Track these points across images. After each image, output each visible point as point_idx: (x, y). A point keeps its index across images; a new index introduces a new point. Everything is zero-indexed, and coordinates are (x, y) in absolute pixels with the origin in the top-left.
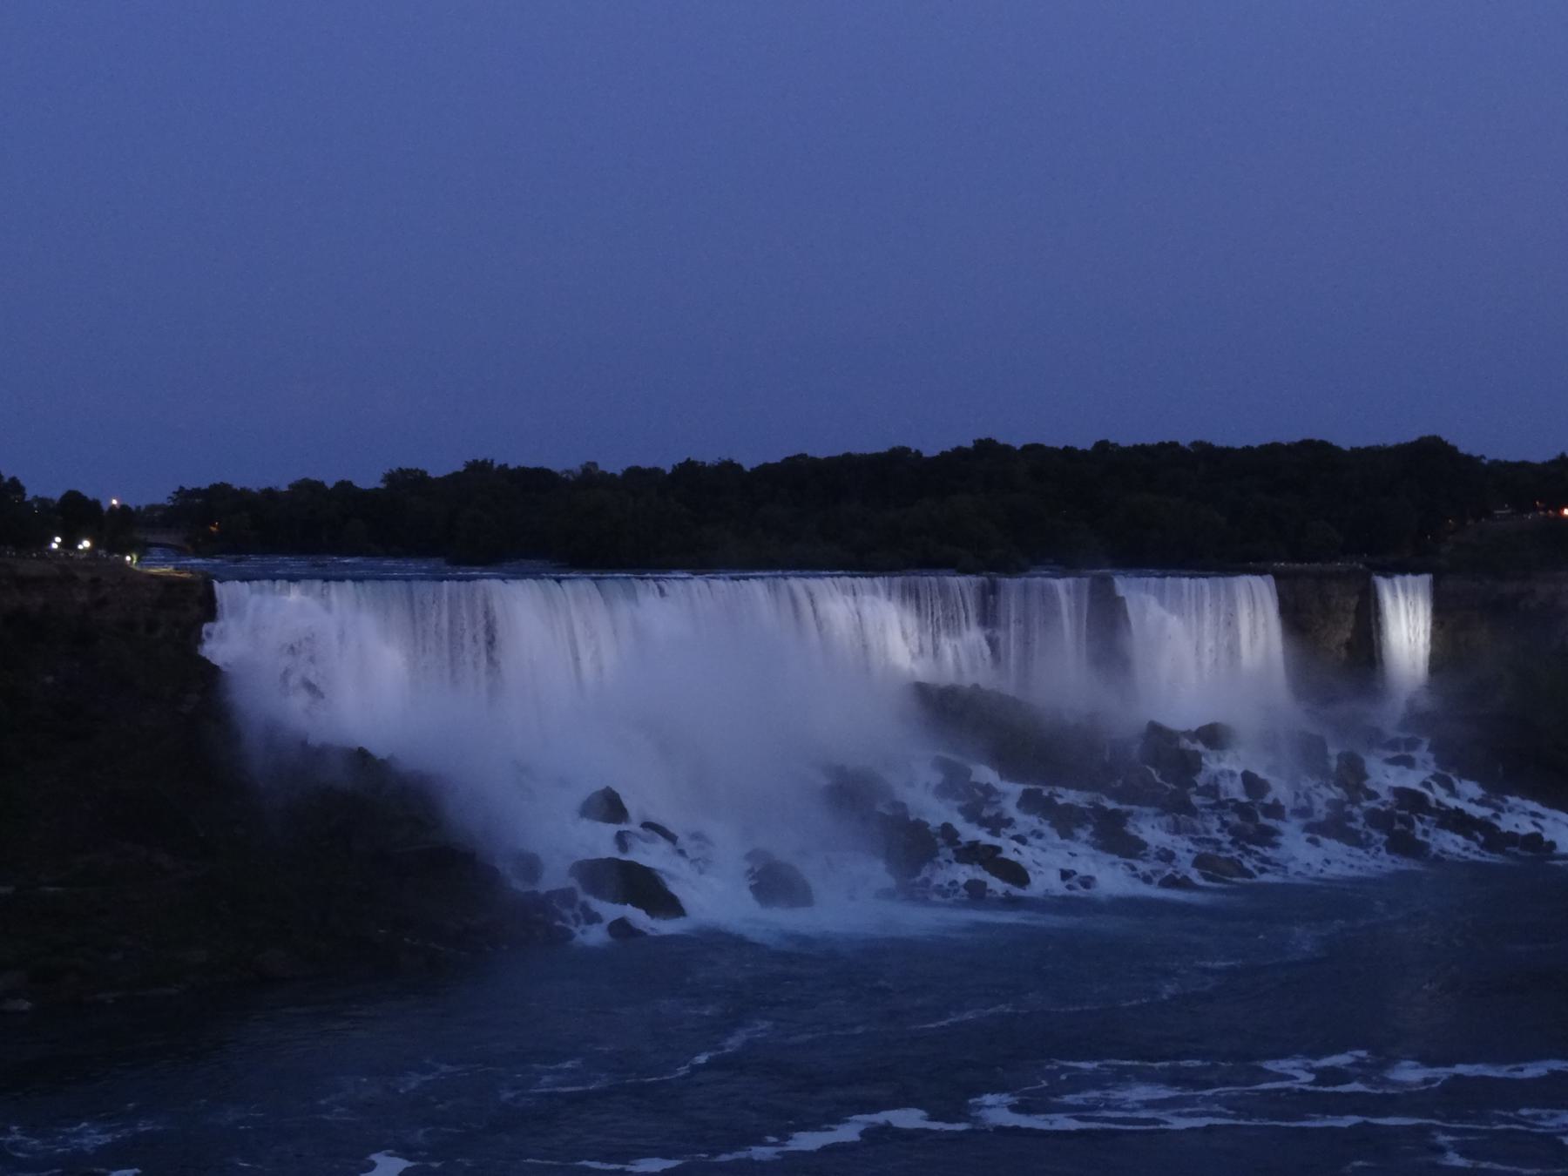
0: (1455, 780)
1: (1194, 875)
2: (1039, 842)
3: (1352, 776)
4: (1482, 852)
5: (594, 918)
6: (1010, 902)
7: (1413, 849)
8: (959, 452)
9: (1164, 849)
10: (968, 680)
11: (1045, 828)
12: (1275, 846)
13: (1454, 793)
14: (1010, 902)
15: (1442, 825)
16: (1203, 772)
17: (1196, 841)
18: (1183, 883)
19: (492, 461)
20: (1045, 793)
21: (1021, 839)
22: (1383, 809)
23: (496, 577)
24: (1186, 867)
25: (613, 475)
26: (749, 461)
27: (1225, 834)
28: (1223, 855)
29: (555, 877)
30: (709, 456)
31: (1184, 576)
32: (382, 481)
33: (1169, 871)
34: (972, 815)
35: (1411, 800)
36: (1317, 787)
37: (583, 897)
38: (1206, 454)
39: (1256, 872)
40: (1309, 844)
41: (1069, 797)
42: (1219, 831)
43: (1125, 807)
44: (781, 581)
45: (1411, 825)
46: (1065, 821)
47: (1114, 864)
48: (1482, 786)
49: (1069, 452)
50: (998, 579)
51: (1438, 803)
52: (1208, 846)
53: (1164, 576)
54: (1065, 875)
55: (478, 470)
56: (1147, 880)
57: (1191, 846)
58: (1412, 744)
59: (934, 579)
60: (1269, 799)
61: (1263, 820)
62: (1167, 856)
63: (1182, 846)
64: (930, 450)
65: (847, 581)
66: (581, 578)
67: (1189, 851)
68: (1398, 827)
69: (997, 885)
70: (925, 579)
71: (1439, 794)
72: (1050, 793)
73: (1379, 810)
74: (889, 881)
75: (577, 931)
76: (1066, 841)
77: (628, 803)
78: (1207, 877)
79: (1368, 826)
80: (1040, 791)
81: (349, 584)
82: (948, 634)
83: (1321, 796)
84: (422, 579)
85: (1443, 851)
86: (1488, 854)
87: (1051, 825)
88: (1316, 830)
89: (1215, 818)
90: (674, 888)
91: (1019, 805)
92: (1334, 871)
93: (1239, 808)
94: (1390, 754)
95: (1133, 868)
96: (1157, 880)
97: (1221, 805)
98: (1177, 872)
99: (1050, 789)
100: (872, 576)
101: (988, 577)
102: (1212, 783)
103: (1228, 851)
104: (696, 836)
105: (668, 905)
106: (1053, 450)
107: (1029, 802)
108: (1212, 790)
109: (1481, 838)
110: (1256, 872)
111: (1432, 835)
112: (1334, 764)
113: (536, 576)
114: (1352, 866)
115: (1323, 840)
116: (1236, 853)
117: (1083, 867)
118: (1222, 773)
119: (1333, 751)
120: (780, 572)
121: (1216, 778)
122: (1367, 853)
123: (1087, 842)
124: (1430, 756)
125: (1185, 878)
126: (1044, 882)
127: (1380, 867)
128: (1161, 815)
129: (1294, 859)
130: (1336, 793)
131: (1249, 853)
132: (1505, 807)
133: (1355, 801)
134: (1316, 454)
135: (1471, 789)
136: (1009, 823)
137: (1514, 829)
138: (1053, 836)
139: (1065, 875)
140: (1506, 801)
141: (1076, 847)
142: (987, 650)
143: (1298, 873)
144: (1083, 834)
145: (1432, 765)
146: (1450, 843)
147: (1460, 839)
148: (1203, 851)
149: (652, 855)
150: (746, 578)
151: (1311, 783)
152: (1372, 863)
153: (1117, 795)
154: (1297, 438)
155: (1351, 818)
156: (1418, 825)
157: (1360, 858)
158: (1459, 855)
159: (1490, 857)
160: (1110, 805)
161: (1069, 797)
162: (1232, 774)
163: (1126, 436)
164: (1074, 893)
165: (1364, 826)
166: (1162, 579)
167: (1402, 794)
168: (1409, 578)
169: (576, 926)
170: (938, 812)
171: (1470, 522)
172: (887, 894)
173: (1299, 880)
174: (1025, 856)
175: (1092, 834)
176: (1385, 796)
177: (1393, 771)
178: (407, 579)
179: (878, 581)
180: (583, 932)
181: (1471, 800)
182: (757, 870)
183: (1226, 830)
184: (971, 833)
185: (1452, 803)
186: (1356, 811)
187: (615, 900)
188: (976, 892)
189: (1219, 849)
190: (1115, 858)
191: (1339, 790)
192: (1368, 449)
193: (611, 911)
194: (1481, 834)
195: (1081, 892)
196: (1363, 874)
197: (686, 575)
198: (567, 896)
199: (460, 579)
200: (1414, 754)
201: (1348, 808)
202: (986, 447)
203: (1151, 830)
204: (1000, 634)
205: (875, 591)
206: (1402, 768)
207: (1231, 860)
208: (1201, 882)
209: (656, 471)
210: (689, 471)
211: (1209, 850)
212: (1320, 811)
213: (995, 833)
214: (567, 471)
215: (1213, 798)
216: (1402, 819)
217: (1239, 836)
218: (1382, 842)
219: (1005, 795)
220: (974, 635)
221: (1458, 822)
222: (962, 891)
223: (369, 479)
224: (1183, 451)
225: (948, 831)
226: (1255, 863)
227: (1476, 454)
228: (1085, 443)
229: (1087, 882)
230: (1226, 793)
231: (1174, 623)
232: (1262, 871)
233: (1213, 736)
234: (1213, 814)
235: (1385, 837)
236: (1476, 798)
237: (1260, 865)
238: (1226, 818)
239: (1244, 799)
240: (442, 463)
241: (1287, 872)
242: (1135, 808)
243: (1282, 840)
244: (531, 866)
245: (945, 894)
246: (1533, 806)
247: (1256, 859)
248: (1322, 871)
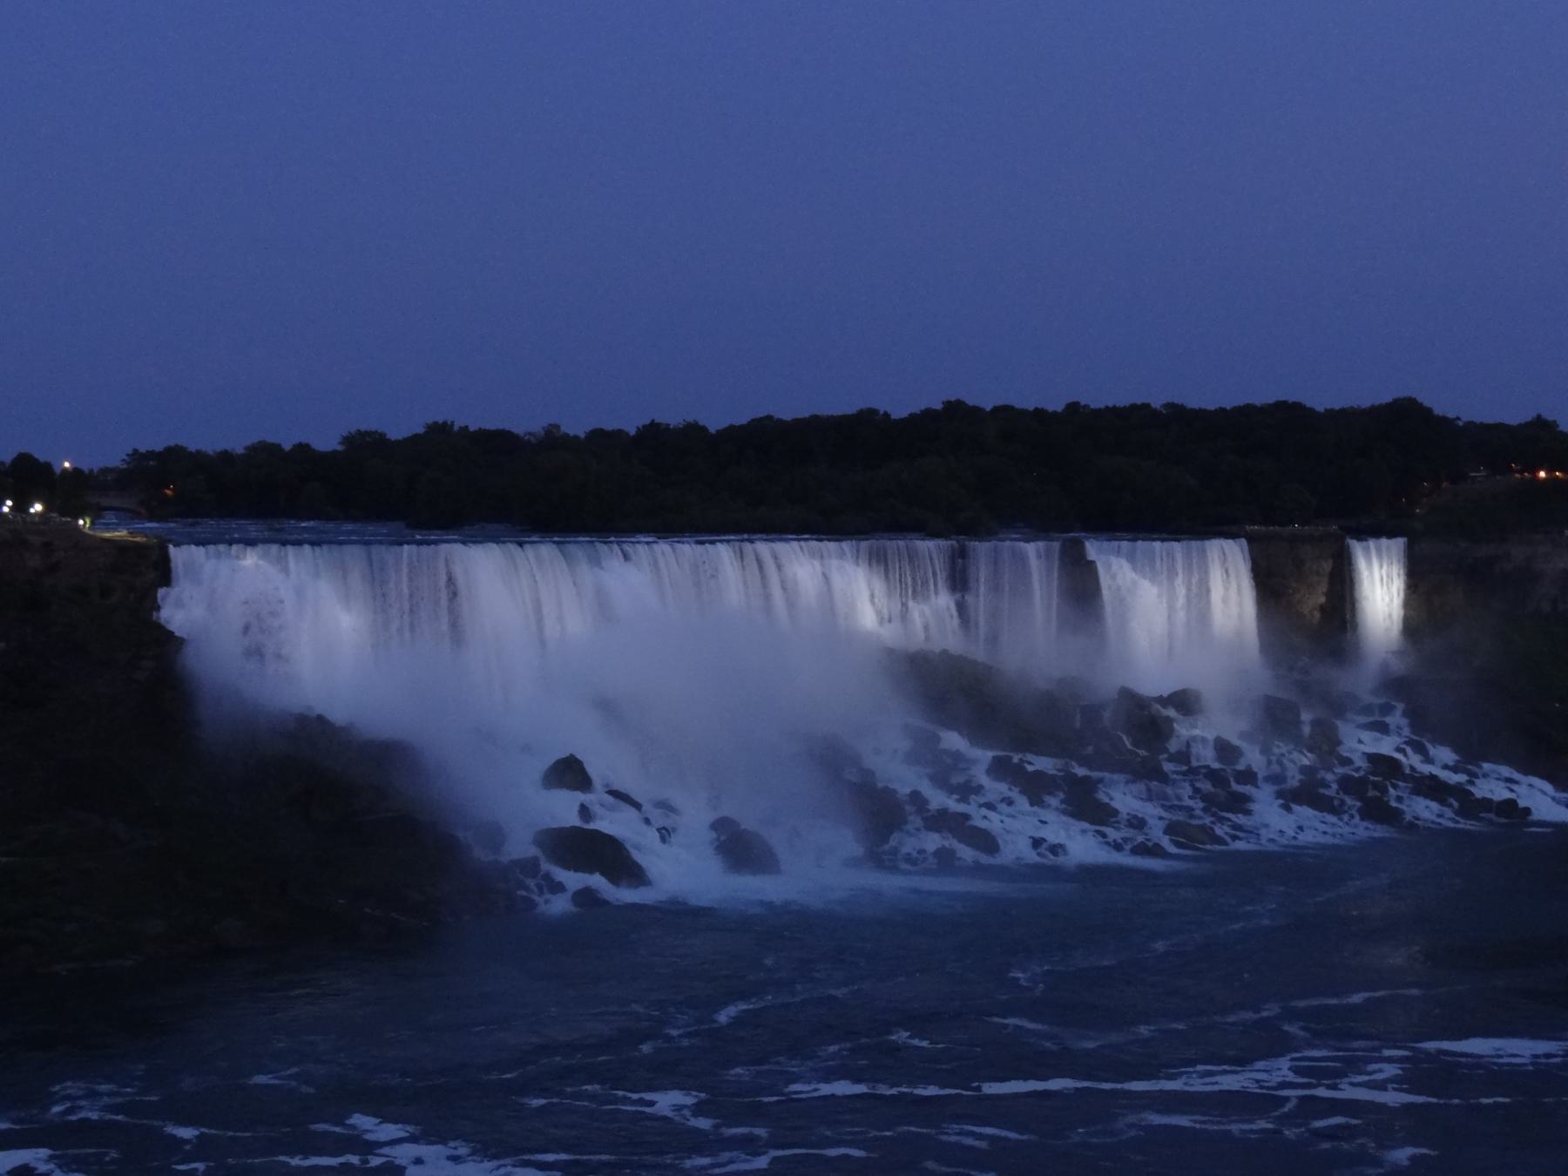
3: (1326, 743)
6: (977, 870)
11: (1015, 794)
30: (673, 418)
34: (941, 780)
35: (1385, 766)
38: (1178, 415)
41: (1042, 764)
46: (1036, 788)
54: (1037, 843)
58: (1387, 709)
62: (1138, 823)
69: (966, 853)
71: (1412, 760)
74: (858, 850)
77: (593, 769)
92: (1307, 838)
93: (1212, 775)
97: (1192, 772)
107: (1000, 769)
108: (1183, 756)
113: (496, 539)
117: (1053, 834)
130: (1306, 759)
134: (1289, 415)
135: (1445, 755)
138: (1023, 803)
139: (1037, 843)
146: (1424, 809)
161: (1042, 764)
170: (904, 777)
174: (993, 822)
184: (938, 799)
195: (1050, 859)
202: (955, 409)
203: (1124, 798)
210: (653, 433)
220: (944, 600)
221: (1432, 788)
223: (326, 441)
225: (916, 798)
229: (1056, 849)
233: (1184, 702)
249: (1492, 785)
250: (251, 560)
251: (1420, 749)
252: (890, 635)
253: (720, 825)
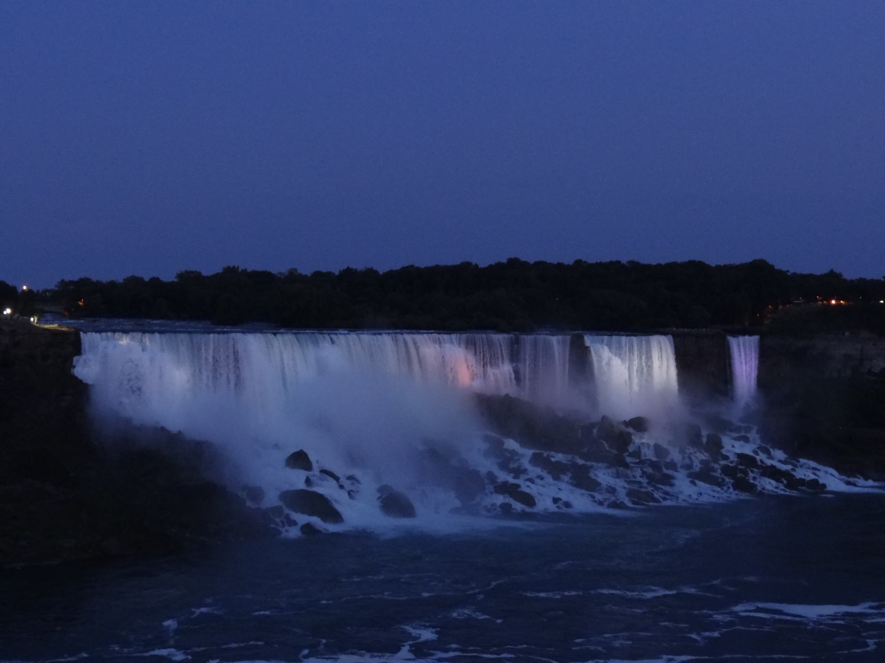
0: (771, 450)
1: (627, 502)
2: (540, 482)
3: (714, 446)
4: (786, 489)
5: (293, 523)
6: (523, 516)
7: (747, 487)
8: (499, 265)
9: (610, 487)
10: (504, 391)
11: (544, 474)
12: (672, 485)
13: (770, 457)
14: (523, 516)
15: (763, 474)
16: (632, 444)
17: (629, 482)
18: (620, 506)
19: (238, 268)
20: (545, 455)
21: (531, 480)
22: (731, 465)
23: (239, 332)
24: (622, 496)
25: (306, 275)
26: (382, 269)
27: (645, 478)
28: (644, 490)
29: (271, 499)
30: (359, 265)
31: (623, 335)
32: (176, 278)
33: (613, 499)
34: (504, 466)
36: (695, 453)
37: (287, 511)
38: (635, 267)
39: (661, 500)
40: (690, 484)
41: (558, 457)
42: (641, 477)
43: (589, 463)
44: (399, 336)
45: (746, 474)
46: (556, 471)
47: (582, 494)
48: (785, 452)
49: (560, 265)
50: (520, 336)
51: (761, 461)
52: (634, 485)
53: (611, 335)
54: (556, 500)
55: (231, 271)
56: (601, 503)
57: (626, 486)
58: (748, 429)
59: (484, 336)
60: (668, 460)
61: (665, 471)
62: (612, 490)
63: (620, 484)
64: (483, 263)
65: (436, 336)
66: (286, 333)
67: (625, 488)
68: (739, 475)
69: (518, 506)
70: (479, 336)
71: (761, 457)
72: (548, 455)
73: (729, 466)
74: (457, 503)
75: (283, 530)
76: (556, 482)
77: (313, 458)
78: (634, 503)
79: (723, 475)
80: (543, 454)
81: (157, 335)
82: (491, 366)
83: (696, 457)
84: (197, 332)
85: (764, 489)
86: (788, 491)
87: (549, 473)
88: (695, 477)
89: (639, 469)
90: (337, 506)
91: (530, 462)
92: (705, 499)
93: (652, 464)
94: (735, 435)
95: (593, 497)
96: (606, 504)
97: (642, 462)
98: (617, 500)
99: (548, 453)
100: (450, 334)
101: (515, 335)
102: (637, 450)
103: (646, 488)
104: (350, 478)
105: (333, 515)
106: (551, 265)
107: (536, 460)
108: (637, 454)
109: (785, 482)
110: (661, 500)
111: (758, 480)
112: (704, 440)
113: (261, 331)
114: (714, 497)
115: (700, 484)
116: (650, 489)
117: (564, 496)
118: (643, 444)
119: (704, 433)
120: (398, 331)
121: (639, 447)
122: (722, 489)
123: (567, 482)
124: (757, 436)
125: (622, 503)
126: (544, 504)
127: (729, 497)
128: (608, 468)
129: (681, 492)
130: (703, 456)
131: (657, 489)
132: (798, 464)
133: (716, 461)
134: (696, 268)
135: (779, 454)
136: (525, 471)
137: (803, 477)
138: (549, 479)
139: (556, 500)
140: (798, 461)
141: (563, 486)
142: (513, 376)
143: (684, 500)
144: (566, 478)
145: (758, 442)
146: (769, 485)
147: (773, 482)
148: (632, 488)
149: (326, 489)
150: (380, 334)
151: (692, 450)
152: (725, 495)
153: (584, 456)
154: (686, 260)
155: (714, 470)
156: (751, 475)
157: (718, 492)
158: (773, 491)
159: (790, 492)
160: (580, 462)
161: (558, 457)
162: (648, 445)
163: (592, 257)
164: (560, 511)
165: (721, 475)
166: (610, 337)
167: (741, 456)
168: (747, 338)
169: (283, 528)
170: (486, 465)
171: (780, 307)
172: (455, 511)
173: (684, 504)
175: (571, 478)
176: (732, 458)
177: (737, 444)
178: (190, 333)
179: (454, 336)
180: (287, 531)
181: (780, 461)
182: (384, 496)
183: (645, 476)
184: (503, 476)
185: (769, 462)
186: (716, 466)
187: (303, 512)
188: (506, 509)
189: (641, 487)
190: (583, 491)
191: (707, 454)
192: (725, 266)
193: (302, 519)
194: (785, 479)
195: (564, 510)
196: (720, 501)
197: (346, 332)
198: (278, 511)
199: (219, 333)
200: (749, 435)
201: (712, 464)
202: (514, 263)
203: (603, 476)
204: (520, 365)
205: (452, 342)
206: (742, 442)
207: (647, 493)
208: (630, 505)
209: (329, 274)
211: (635, 487)
212: (697, 466)
213: (516, 477)
214: (280, 273)
215: (637, 458)
216: (741, 471)
217: (651, 479)
218: (731, 483)
219: (523, 456)
220: (506, 368)
221: (773, 473)
222: (498, 509)
223: (169, 276)
224: (623, 266)
225: (491, 477)
226: (661, 494)
227: (784, 269)
228: (568, 260)
229: (568, 505)
230: (645, 456)
231: (616, 362)
232: (665, 499)
233: (638, 424)
234: (637, 467)
235: (732, 481)
236: (783, 459)
237: (663, 496)
238: (645, 470)
239: (654, 459)
240: (210, 268)
241: (678, 500)
242: (595, 464)
243: (675, 482)
244: (256, 494)
245: (489, 510)
246: (813, 464)
247: (661, 492)
248: (697, 499)
249: (805, 470)
251: (767, 451)
252: (477, 385)
253: (382, 489)
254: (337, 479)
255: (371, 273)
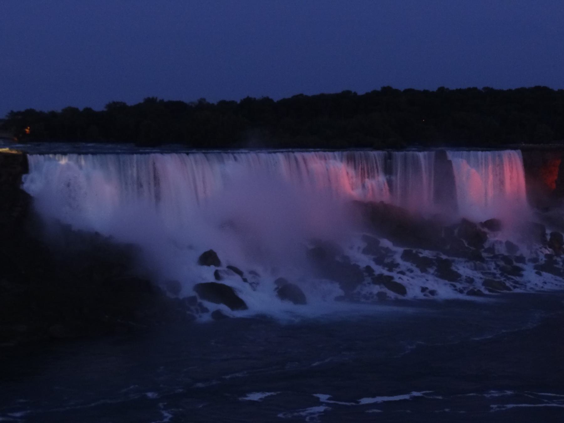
6: (397, 302)
11: (414, 268)
14: (397, 302)
30: (257, 95)
34: (379, 261)
41: (426, 253)
54: (424, 290)
55: (150, 102)
62: (470, 281)
69: (391, 294)
77: (221, 256)
92: (547, 287)
97: (495, 257)
105: (238, 303)
107: (406, 256)
108: (491, 250)
130: (548, 251)
138: (417, 271)
139: (424, 290)
149: (230, 281)
161: (426, 253)
174: (404, 280)
184: (379, 270)
193: (211, 306)
198: (192, 300)
202: (387, 90)
210: (248, 101)
220: (381, 178)
223: (99, 106)
225: (369, 269)
229: (433, 293)
250: (64, 161)
252: (357, 193)
253: (277, 282)
254: (240, 273)
255: (267, 101)
